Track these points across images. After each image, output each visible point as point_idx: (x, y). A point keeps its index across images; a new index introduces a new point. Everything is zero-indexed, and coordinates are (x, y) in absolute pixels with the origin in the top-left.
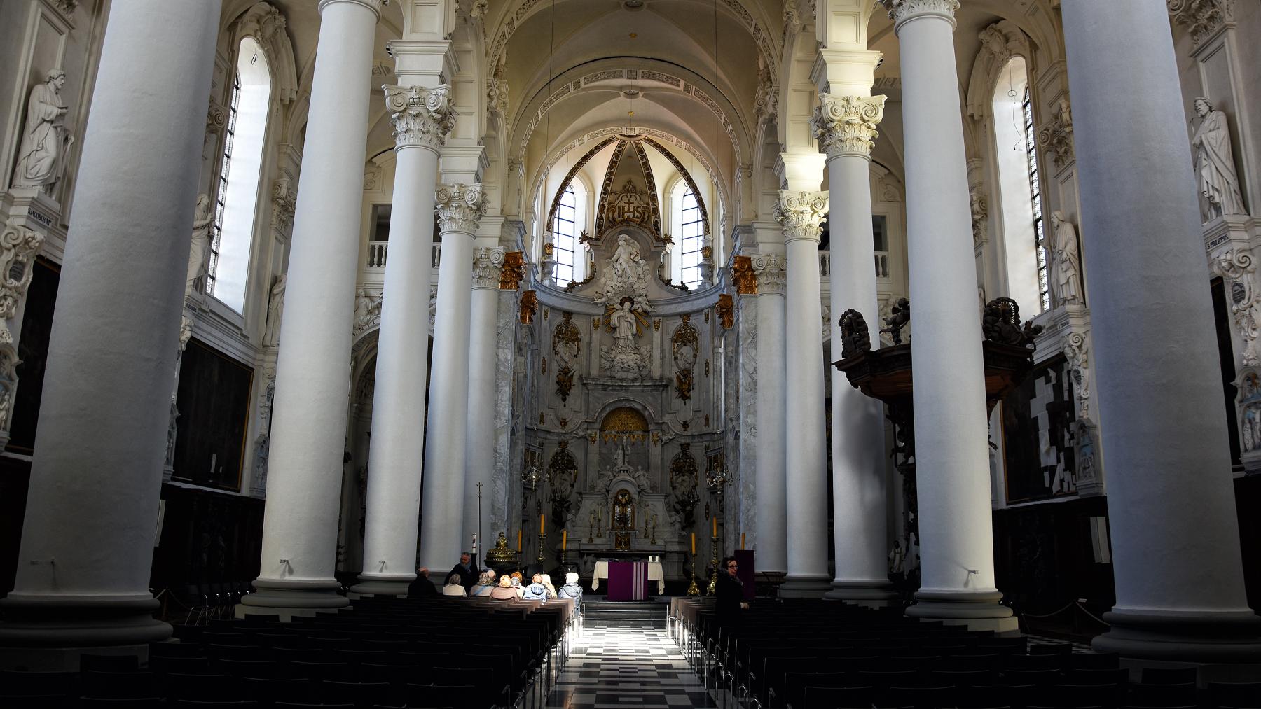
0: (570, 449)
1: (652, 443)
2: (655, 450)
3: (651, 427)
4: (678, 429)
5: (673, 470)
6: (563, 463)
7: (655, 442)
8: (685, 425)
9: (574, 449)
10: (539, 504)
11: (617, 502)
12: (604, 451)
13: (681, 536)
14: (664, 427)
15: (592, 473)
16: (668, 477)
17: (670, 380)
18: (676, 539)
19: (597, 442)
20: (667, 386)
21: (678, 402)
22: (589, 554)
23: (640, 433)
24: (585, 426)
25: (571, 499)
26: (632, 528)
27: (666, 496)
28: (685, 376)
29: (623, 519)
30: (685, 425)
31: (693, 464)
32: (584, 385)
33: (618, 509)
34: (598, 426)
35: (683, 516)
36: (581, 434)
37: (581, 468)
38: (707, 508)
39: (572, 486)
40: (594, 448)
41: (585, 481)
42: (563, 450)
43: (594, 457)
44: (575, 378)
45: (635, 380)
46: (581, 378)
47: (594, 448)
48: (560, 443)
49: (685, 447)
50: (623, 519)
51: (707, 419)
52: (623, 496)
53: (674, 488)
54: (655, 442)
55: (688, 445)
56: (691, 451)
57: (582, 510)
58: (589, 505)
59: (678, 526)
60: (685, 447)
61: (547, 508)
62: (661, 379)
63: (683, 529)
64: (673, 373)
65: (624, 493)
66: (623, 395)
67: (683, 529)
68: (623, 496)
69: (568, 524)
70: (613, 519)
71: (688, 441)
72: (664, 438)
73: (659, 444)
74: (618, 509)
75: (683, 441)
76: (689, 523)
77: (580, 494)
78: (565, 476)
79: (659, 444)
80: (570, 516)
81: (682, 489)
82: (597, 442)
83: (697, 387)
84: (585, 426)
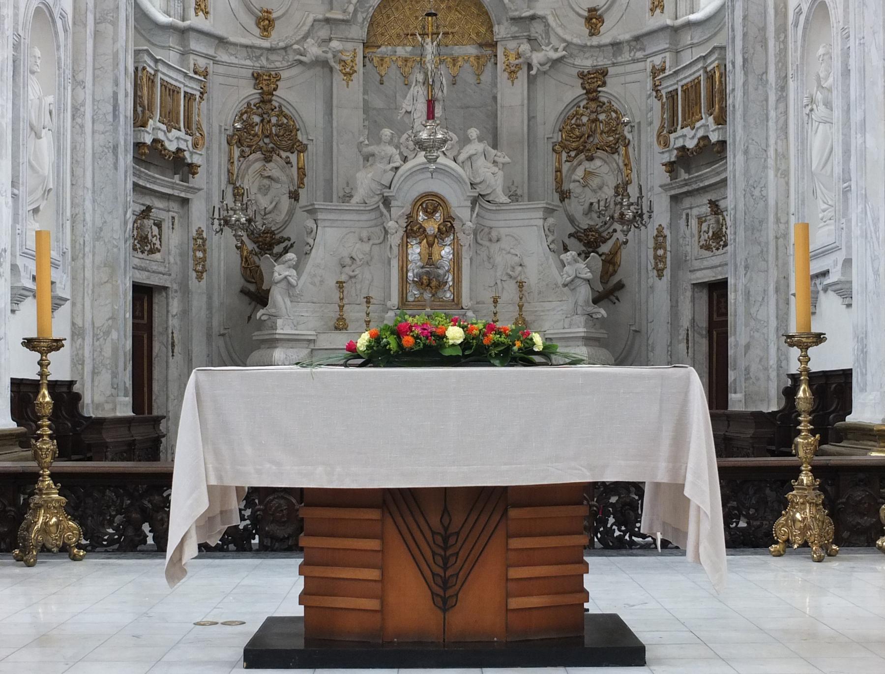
0: (284, 94)
1: (503, 76)
2: (512, 95)
3: (501, 31)
4: (577, 32)
5: (559, 148)
6: (267, 132)
7: (512, 73)
9: (296, 95)
10: (200, 242)
12: (378, 102)
14: (537, 29)
15: (345, 155)
16: (546, 162)
18: (580, 330)
19: (358, 78)
23: (472, 50)
24: (324, 33)
26: (456, 303)
27: (549, 211)
29: (430, 281)
30: (594, 19)
31: (615, 127)
33: (415, 251)
34: (359, 32)
36: (313, 50)
37: (316, 149)
38: (659, 240)
39: (294, 196)
40: (350, 94)
41: (329, 182)
42: (266, 98)
43: (349, 117)
47: (350, 94)
50: (430, 281)
52: (430, 213)
53: (564, 195)
54: (512, 73)
55: (604, 73)
56: (612, 89)
57: (318, 255)
58: (333, 241)
59: (584, 293)
60: (593, 81)
61: (224, 252)
63: (596, 301)
65: (431, 203)
68: (430, 213)
69: (277, 296)
70: (403, 279)
71: (602, 61)
72: (537, 58)
73: (522, 75)
74: (415, 251)
75: (587, 63)
77: (312, 212)
78: (273, 169)
79: (522, 75)
81: (590, 197)
82: (358, 78)
84: (324, 33)
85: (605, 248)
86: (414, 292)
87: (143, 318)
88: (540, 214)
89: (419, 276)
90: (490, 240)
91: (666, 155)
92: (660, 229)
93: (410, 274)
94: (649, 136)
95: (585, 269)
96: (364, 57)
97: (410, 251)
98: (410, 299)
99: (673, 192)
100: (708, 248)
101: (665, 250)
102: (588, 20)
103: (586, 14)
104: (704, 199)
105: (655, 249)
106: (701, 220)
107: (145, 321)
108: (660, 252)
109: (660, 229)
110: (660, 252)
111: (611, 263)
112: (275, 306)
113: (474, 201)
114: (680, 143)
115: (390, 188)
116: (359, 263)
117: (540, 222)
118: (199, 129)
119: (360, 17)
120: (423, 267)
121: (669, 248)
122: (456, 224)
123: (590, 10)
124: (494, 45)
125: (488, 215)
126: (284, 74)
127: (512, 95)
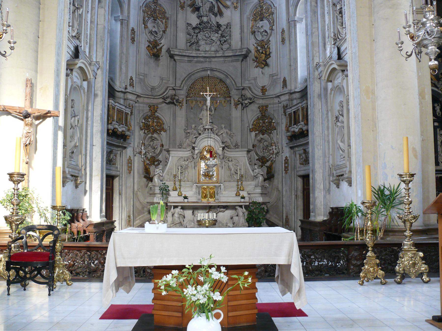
8: (264, 90)
11: (203, 158)
13: (263, 187)
17: (249, 51)
20: (245, 57)
21: (256, 72)
22: (175, 207)
25: (160, 158)
27: (249, 151)
28: (263, 47)
32: (172, 56)
35: (265, 169)
40: (181, 114)
44: (164, 50)
45: (216, 51)
46: (168, 51)
48: (150, 106)
49: (263, 109)
51: (285, 81)
59: (261, 178)
62: (241, 49)
64: (251, 44)
66: (207, 65)
67: (265, 180)
69: (156, 179)
76: (270, 176)
77: (168, 151)
80: (158, 171)
83: (273, 55)
85: (268, 164)
86: (202, 178)
87: (110, 186)
88: (246, 153)
89: (203, 172)
90: (229, 161)
91: (288, 134)
92: (286, 157)
93: (201, 172)
94: (283, 127)
95: (261, 172)
96: (186, 101)
97: (201, 164)
98: (201, 180)
99: (291, 146)
100: (302, 164)
101: (288, 164)
102: (262, 90)
103: (261, 88)
104: (301, 148)
105: (285, 164)
106: (300, 155)
107: (110, 187)
108: (286, 165)
109: (286, 157)
110: (286, 165)
111: (270, 169)
112: (155, 182)
113: (223, 148)
114: (293, 129)
115: (194, 143)
116: (184, 168)
117: (246, 155)
118: (130, 124)
119: (185, 88)
120: (206, 170)
121: (289, 164)
122: (218, 156)
123: (263, 87)
124: (230, 97)
125: (228, 153)
126: (159, 106)
127: (236, 113)
